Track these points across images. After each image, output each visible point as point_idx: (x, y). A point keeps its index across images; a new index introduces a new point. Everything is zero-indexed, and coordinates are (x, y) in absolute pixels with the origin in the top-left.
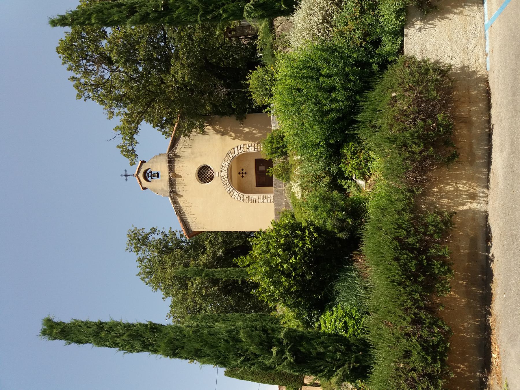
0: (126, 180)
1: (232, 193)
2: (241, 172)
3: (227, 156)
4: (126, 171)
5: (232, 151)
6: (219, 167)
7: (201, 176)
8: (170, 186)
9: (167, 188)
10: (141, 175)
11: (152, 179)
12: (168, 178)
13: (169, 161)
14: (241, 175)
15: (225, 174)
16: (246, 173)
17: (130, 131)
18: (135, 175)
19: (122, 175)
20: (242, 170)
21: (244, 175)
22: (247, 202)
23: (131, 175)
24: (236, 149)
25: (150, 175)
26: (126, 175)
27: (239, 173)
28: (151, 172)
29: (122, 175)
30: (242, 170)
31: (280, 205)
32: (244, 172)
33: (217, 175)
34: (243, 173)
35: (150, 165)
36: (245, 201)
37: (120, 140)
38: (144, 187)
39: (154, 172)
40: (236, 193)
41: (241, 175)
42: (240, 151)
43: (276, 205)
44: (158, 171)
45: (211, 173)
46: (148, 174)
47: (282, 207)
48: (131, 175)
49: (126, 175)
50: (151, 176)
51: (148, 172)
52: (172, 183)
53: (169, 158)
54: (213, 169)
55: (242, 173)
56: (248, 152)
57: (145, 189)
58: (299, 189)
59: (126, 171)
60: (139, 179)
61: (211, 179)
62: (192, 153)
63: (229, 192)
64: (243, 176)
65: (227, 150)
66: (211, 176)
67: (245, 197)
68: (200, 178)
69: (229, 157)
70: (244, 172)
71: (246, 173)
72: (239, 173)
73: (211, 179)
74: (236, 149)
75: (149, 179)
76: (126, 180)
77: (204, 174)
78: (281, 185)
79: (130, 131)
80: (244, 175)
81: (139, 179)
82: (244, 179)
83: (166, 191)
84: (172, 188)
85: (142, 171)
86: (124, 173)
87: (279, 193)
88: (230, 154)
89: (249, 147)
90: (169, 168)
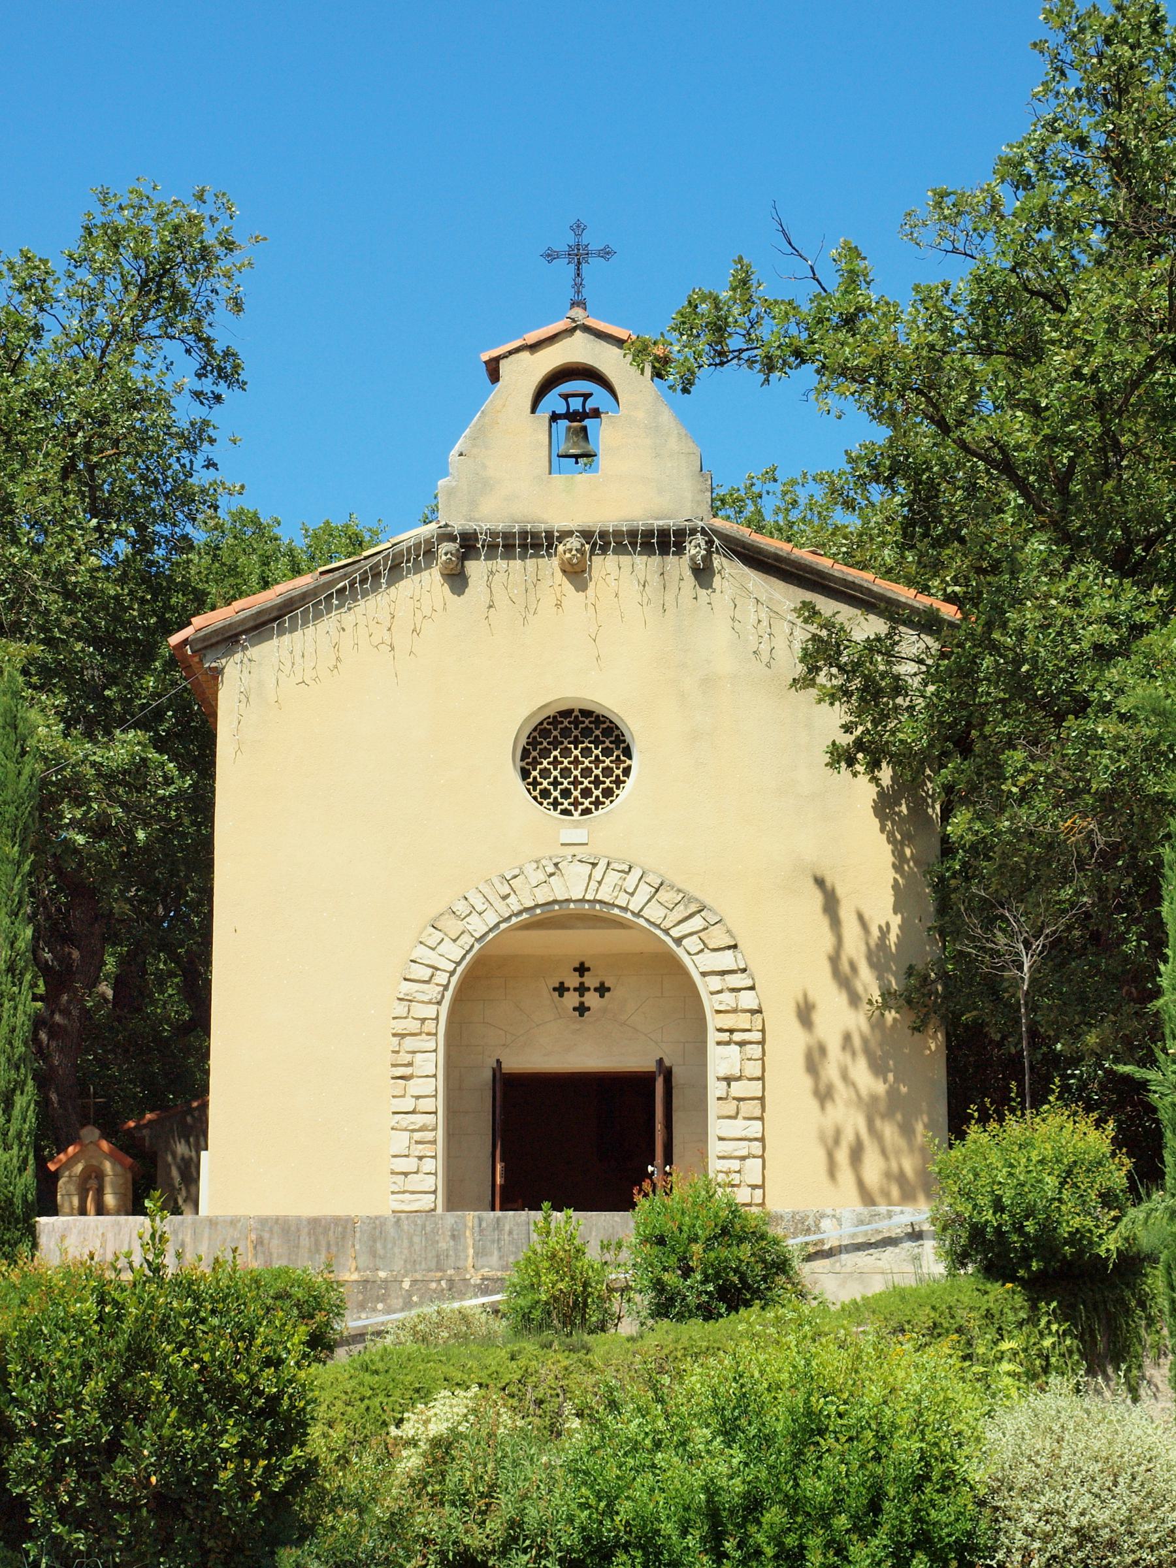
0: (551, 256)
1: (452, 926)
2: (591, 981)
3: (687, 899)
4: (606, 253)
5: (718, 937)
6: (619, 852)
7: (565, 732)
8: (507, 536)
9: (492, 515)
10: (578, 350)
11: (555, 417)
12: (558, 523)
13: (664, 533)
14: (573, 981)
15: (573, 885)
16: (582, 1009)
17: (835, 342)
18: (577, 313)
19: (578, 228)
20: (602, 990)
21: (572, 999)
22: (400, 1026)
23: (578, 287)
24: (726, 960)
25: (576, 404)
26: (578, 256)
27: (582, 969)
28: (596, 413)
29: (578, 228)
30: (602, 990)
31: (373, 1254)
32: (591, 999)
33: (573, 829)
34: (582, 989)
35: (640, 415)
36: (401, 1009)
37: (783, 283)
38: (502, 363)
39: (606, 435)
40: (457, 954)
41: (573, 981)
42: (715, 983)
43: (376, 1227)
44: (603, 460)
45: (586, 793)
46: (586, 396)
47: (363, 1260)
48: (578, 287)
49: (578, 256)
50: (571, 416)
52: (529, 543)
53: (681, 534)
54: (609, 807)
55: (582, 985)
56: (713, 1036)
57: (493, 370)
58: (437, 1428)
59: (606, 253)
61: (545, 794)
62: (708, 683)
63: (461, 907)
64: (561, 989)
65: (728, 904)
66: (566, 793)
67: (431, 1011)
68: (554, 720)
69: (680, 912)
70: (591, 999)
71: (582, 1009)
72: (582, 969)
73: (545, 794)
74: (726, 960)
75: (553, 402)
76: (551, 256)
77: (573, 749)
78: (494, 1260)
79: (835, 342)
80: (572, 999)
82: (547, 996)
84: (493, 547)
85: (608, 360)
86: (593, 240)
87: (444, 1244)
88: (697, 923)
89: (741, 1044)
90: (617, 533)
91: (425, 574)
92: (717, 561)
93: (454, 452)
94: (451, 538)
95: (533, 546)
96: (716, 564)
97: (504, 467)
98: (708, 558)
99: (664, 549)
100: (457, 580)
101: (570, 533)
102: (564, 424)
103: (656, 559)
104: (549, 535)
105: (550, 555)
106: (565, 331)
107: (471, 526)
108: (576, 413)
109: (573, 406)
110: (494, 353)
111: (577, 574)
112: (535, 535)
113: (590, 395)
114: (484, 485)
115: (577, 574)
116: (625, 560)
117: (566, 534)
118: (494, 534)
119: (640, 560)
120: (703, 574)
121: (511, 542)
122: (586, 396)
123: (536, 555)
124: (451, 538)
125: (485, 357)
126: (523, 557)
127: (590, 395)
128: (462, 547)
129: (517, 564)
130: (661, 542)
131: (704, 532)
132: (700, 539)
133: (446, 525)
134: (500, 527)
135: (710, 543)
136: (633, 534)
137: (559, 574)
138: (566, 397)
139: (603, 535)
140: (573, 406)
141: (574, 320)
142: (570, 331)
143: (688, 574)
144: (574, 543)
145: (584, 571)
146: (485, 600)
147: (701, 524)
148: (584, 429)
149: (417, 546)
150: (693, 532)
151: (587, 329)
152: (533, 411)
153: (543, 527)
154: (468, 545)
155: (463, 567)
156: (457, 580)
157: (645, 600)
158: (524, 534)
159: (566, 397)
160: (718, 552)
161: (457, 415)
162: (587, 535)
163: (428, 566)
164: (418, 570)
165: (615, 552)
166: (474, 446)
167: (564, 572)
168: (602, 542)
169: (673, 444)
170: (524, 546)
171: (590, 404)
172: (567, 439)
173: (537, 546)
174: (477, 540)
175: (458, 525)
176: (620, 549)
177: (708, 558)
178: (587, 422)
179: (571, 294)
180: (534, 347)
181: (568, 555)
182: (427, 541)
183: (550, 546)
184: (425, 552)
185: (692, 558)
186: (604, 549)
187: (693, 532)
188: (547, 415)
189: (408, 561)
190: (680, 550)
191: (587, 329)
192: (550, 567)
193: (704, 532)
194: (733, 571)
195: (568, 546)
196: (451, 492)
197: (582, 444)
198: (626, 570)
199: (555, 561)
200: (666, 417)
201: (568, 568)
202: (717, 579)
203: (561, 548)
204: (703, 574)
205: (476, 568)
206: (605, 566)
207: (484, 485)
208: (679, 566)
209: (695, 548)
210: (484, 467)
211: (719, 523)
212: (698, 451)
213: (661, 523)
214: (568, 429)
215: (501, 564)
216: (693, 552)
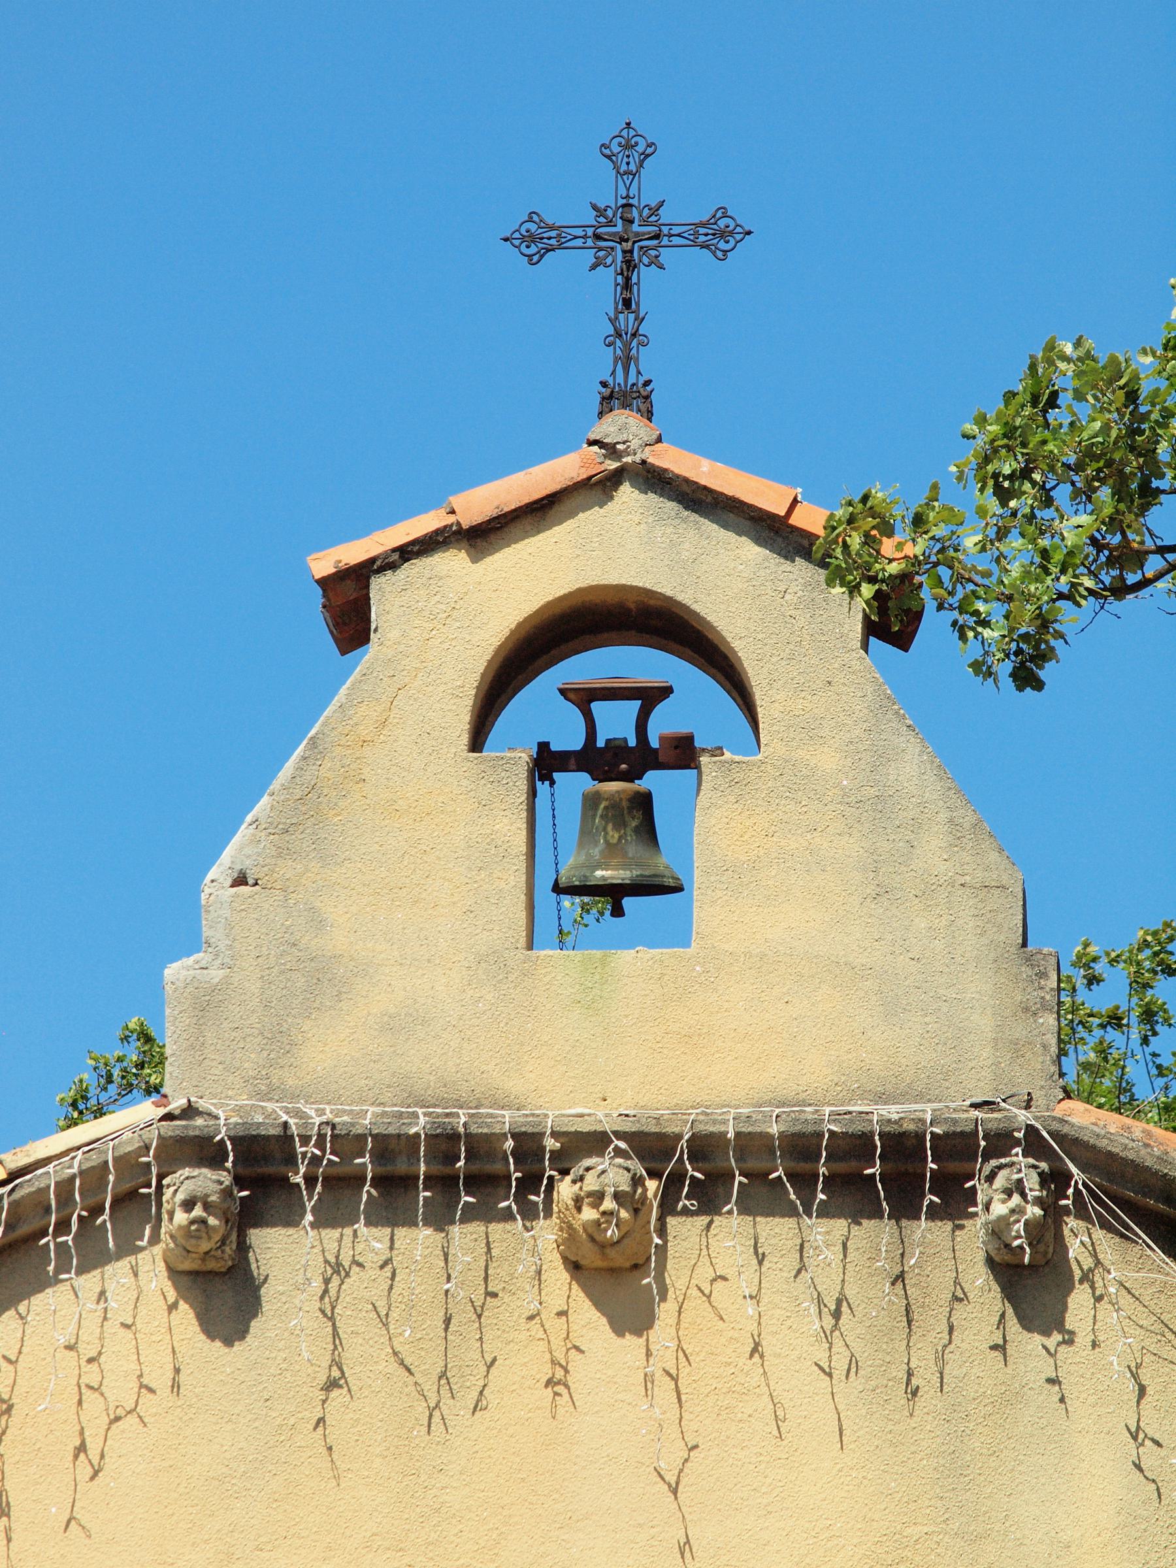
0: (537, 240)
4: (718, 235)
8: (388, 1147)
9: (339, 1076)
10: (624, 546)
11: (546, 763)
13: (902, 1146)
18: (623, 426)
23: (626, 341)
25: (616, 722)
26: (627, 241)
28: (683, 753)
29: (628, 152)
35: (827, 760)
46: (651, 697)
48: (626, 341)
49: (627, 241)
50: (598, 759)
51: (693, 704)
52: (462, 1172)
57: (348, 610)
59: (718, 235)
60: (541, 511)
81: (541, 511)
83: (280, 1041)
85: (720, 579)
86: (676, 190)
90: (750, 1144)
91: (118, 1272)
92: (1080, 1240)
93: (219, 872)
94: (206, 1152)
95: (474, 1182)
96: (1075, 1249)
97: (383, 925)
98: (1047, 1233)
99: (905, 1207)
100: (223, 1292)
101: (596, 1142)
102: (574, 785)
103: (876, 1234)
104: (528, 1145)
105: (529, 1213)
106: (585, 485)
107: (267, 1115)
108: (616, 748)
109: (611, 735)
110: (354, 553)
111: (618, 1277)
112: (481, 1146)
113: (665, 692)
114: (317, 980)
115: (618, 1277)
116: (777, 1231)
117: (585, 1144)
118: (345, 1141)
119: (826, 1233)
120: (1032, 1282)
121: (401, 1167)
122: (651, 697)
123: (484, 1213)
124: (206, 1152)
125: (323, 565)
126: (440, 1219)
127: (665, 692)
128: (240, 1181)
129: (419, 1240)
130: (890, 1173)
131: (1034, 1143)
132: (1022, 1167)
133: (190, 1111)
134: (368, 1118)
135: (1055, 1180)
136: (801, 1146)
137: (558, 1276)
138: (583, 698)
139: (704, 1147)
140: (611, 735)
141: (611, 450)
142: (599, 487)
143: (979, 1280)
144: (609, 1173)
145: (638, 1267)
146: (313, 1355)
147: (1023, 1117)
148: (644, 803)
149: (94, 1177)
150: (1000, 1143)
151: (655, 480)
152: (477, 742)
153: (507, 1119)
154: (263, 1175)
155: (243, 1248)
156: (223, 1292)
157: (840, 1364)
158: (445, 1142)
159: (583, 698)
160: (1081, 1212)
161: (229, 751)
162: (651, 1148)
163: (128, 1248)
164: (93, 1256)
165: (746, 1208)
166: (282, 852)
167: (575, 1267)
168: (697, 1170)
169: (934, 853)
170: (444, 1183)
171: (664, 723)
172: (586, 833)
173: (485, 1182)
174: (291, 1160)
175: (228, 1109)
176: (763, 1198)
177: (1047, 1233)
178: (652, 781)
179: (601, 364)
180: (482, 537)
181: (589, 1214)
182: (128, 1164)
183: (530, 1182)
184: (117, 1203)
185: (998, 1231)
186: (708, 1198)
187: (1000, 1143)
188: (523, 757)
189: (63, 1226)
190: (955, 1201)
191: (655, 480)
192: (529, 1249)
193: (1034, 1143)
194: (1132, 1277)
195: (591, 1183)
196: (206, 1003)
197: (634, 849)
198: (781, 1264)
199: (547, 1233)
200: (912, 768)
201: (590, 1257)
202: (1079, 1300)
203: (565, 1190)
204: (1032, 1282)
205: (286, 1255)
206: (713, 1254)
207: (317, 980)
208: (952, 1255)
209: (1005, 1198)
210: (318, 922)
211: (1083, 1118)
212: (1014, 880)
213: (892, 1111)
214: (591, 801)
215: (371, 1240)
216: (999, 1209)
